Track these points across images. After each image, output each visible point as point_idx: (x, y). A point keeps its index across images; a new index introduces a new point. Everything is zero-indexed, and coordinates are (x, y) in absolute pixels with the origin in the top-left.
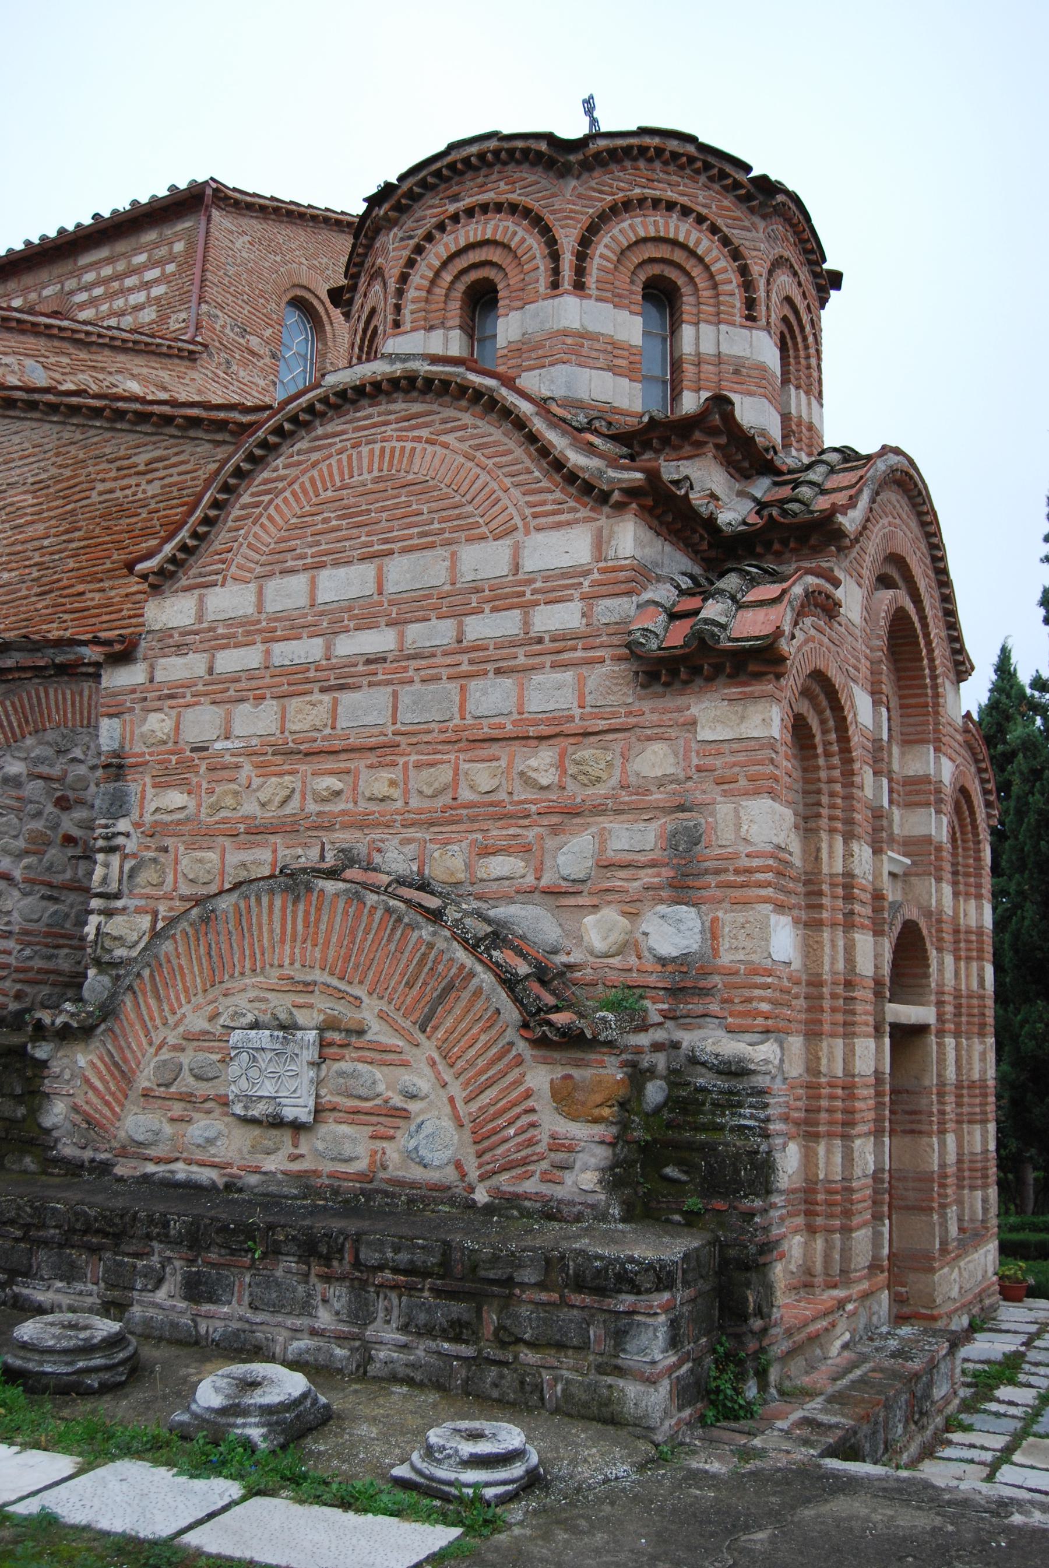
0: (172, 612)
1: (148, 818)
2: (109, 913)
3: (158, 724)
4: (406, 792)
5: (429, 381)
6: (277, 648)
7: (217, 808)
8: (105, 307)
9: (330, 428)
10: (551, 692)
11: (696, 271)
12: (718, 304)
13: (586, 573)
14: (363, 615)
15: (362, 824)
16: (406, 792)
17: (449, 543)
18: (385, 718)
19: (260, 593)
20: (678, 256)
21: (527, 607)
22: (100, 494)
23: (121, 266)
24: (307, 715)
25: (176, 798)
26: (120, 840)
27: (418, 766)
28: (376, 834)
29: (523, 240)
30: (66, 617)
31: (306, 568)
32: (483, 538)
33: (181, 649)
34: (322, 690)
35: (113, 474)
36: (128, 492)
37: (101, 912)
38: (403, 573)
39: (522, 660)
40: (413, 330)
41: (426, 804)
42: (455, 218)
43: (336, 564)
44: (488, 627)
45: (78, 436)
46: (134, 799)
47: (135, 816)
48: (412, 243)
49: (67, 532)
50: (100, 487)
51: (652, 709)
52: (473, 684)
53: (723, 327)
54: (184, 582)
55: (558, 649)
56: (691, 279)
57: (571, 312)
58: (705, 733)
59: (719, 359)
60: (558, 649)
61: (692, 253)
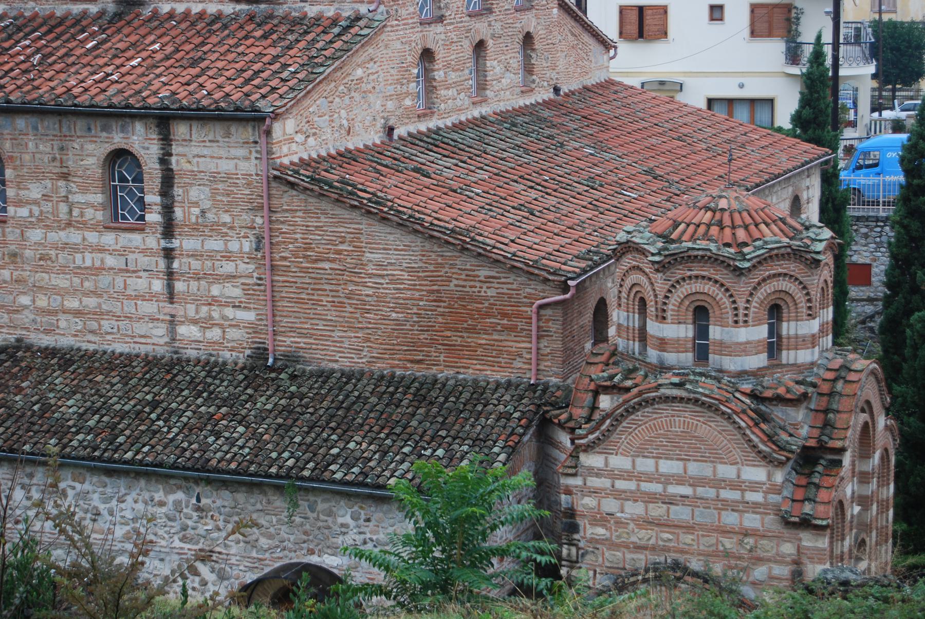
0: (592, 460)
1: (588, 536)
2: (572, 568)
4: (698, 544)
5: (703, 403)
6: (642, 484)
7: (619, 537)
9: (661, 406)
10: (752, 521)
11: (788, 300)
12: (797, 312)
13: (764, 484)
15: (682, 552)
16: (698, 544)
17: (713, 462)
18: (689, 518)
19: (633, 462)
20: (782, 295)
21: (743, 491)
22: (456, 286)
25: (601, 531)
26: (576, 542)
27: (703, 536)
28: (687, 556)
29: (721, 299)
30: (440, 347)
31: (653, 457)
32: (726, 463)
33: (598, 475)
34: (663, 503)
35: (463, 277)
36: (476, 290)
37: (568, 567)
38: (694, 468)
39: (741, 508)
40: (672, 323)
41: (706, 549)
42: (690, 277)
43: (667, 459)
45: (436, 248)
46: (581, 528)
47: (582, 533)
48: (670, 283)
49: (435, 301)
50: (456, 282)
51: (786, 533)
52: (723, 512)
53: (799, 323)
54: (597, 449)
55: (754, 507)
56: (786, 303)
57: (743, 334)
58: (804, 543)
59: (797, 336)
60: (754, 507)
61: (787, 293)
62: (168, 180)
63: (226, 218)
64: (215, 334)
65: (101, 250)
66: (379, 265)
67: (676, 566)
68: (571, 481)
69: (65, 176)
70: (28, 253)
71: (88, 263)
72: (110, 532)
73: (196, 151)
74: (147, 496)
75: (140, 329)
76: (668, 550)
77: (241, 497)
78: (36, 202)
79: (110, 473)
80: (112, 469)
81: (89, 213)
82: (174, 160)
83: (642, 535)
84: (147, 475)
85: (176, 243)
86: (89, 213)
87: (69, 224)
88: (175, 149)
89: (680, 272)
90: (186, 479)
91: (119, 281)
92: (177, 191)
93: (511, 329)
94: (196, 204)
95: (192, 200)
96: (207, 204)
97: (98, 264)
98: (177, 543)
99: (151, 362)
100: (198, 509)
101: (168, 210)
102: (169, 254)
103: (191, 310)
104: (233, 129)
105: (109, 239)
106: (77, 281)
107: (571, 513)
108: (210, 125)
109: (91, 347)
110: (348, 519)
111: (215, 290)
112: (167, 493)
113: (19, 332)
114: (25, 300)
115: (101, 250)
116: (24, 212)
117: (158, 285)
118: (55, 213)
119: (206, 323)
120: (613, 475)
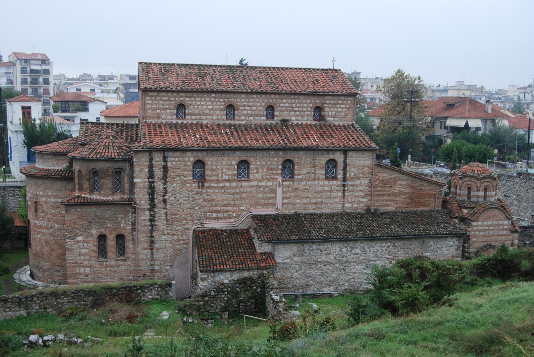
0: (474, 224)
3: (473, 233)
8: (332, 109)
10: (505, 232)
14: (491, 226)
23: (336, 102)
24: (486, 233)
25: (475, 239)
38: (494, 223)
44: (501, 227)
60: (505, 229)
62: (345, 166)
63: (361, 175)
64: (356, 205)
65: (324, 186)
66: (400, 185)
67: (490, 245)
68: (470, 229)
69: (314, 167)
70: (300, 188)
71: (320, 190)
72: (369, 256)
73: (354, 159)
74: (380, 245)
75: (335, 206)
76: (488, 241)
77: (405, 242)
78: (304, 174)
79: (371, 240)
80: (373, 239)
81: (321, 176)
82: (347, 161)
83: (484, 239)
84: (381, 240)
85: (346, 183)
86: (321, 176)
87: (314, 180)
88: (348, 158)
89: (483, 181)
90: (391, 239)
91: (329, 194)
92: (348, 169)
93: (431, 197)
94: (353, 172)
95: (352, 171)
96: (356, 172)
97: (322, 189)
98: (387, 256)
99: (341, 214)
100: (394, 246)
101: (345, 174)
102: (344, 186)
103: (349, 200)
104: (365, 153)
105: (326, 183)
106: (315, 195)
107: (469, 236)
108: (359, 152)
109: (319, 212)
110: (432, 243)
111: (357, 194)
112: (386, 244)
113: (295, 210)
114: (298, 201)
115: (324, 186)
116: (300, 177)
117: (340, 194)
118: (310, 177)
119: (353, 203)
120: (478, 226)
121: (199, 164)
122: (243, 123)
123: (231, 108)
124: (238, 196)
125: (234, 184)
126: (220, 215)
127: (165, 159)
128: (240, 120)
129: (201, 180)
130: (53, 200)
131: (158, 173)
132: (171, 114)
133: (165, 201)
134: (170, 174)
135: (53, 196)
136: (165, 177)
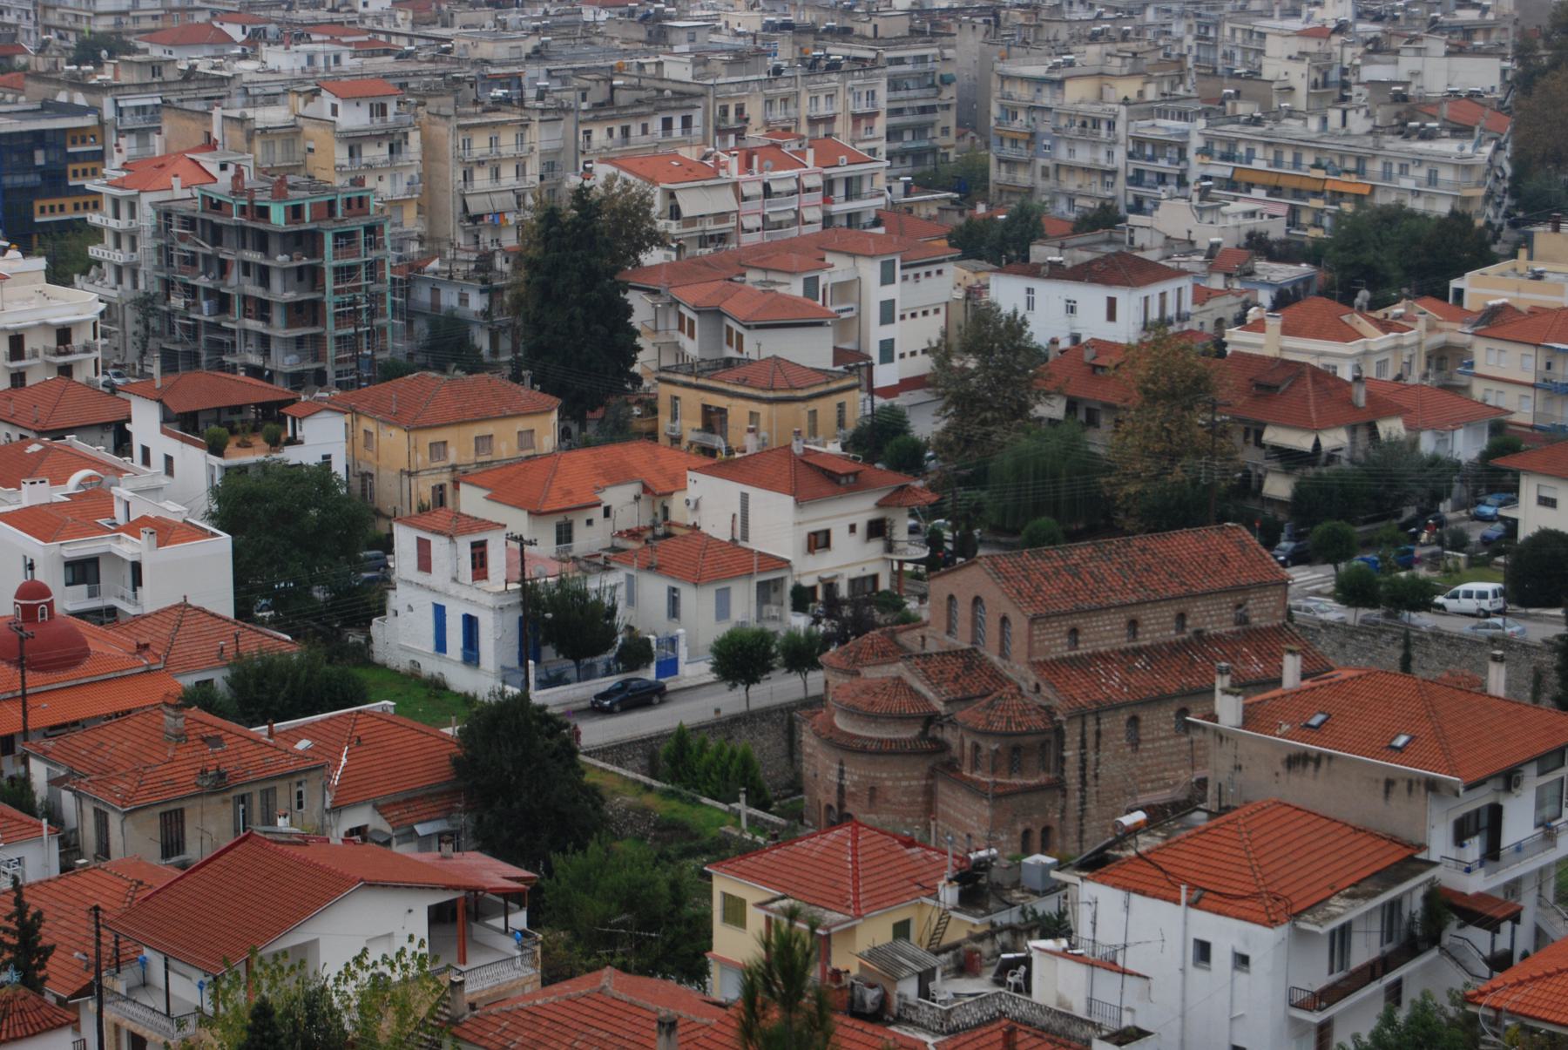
121: (1134, 721)
122: (1148, 643)
123: (1133, 624)
124: (1174, 758)
125: (1172, 742)
126: (1156, 785)
127: (1098, 720)
128: (1145, 640)
129: (1135, 743)
130: (904, 783)
131: (1091, 740)
132: (1062, 644)
133: (1096, 776)
134: (1103, 739)
135: (906, 778)
136: (1098, 744)
